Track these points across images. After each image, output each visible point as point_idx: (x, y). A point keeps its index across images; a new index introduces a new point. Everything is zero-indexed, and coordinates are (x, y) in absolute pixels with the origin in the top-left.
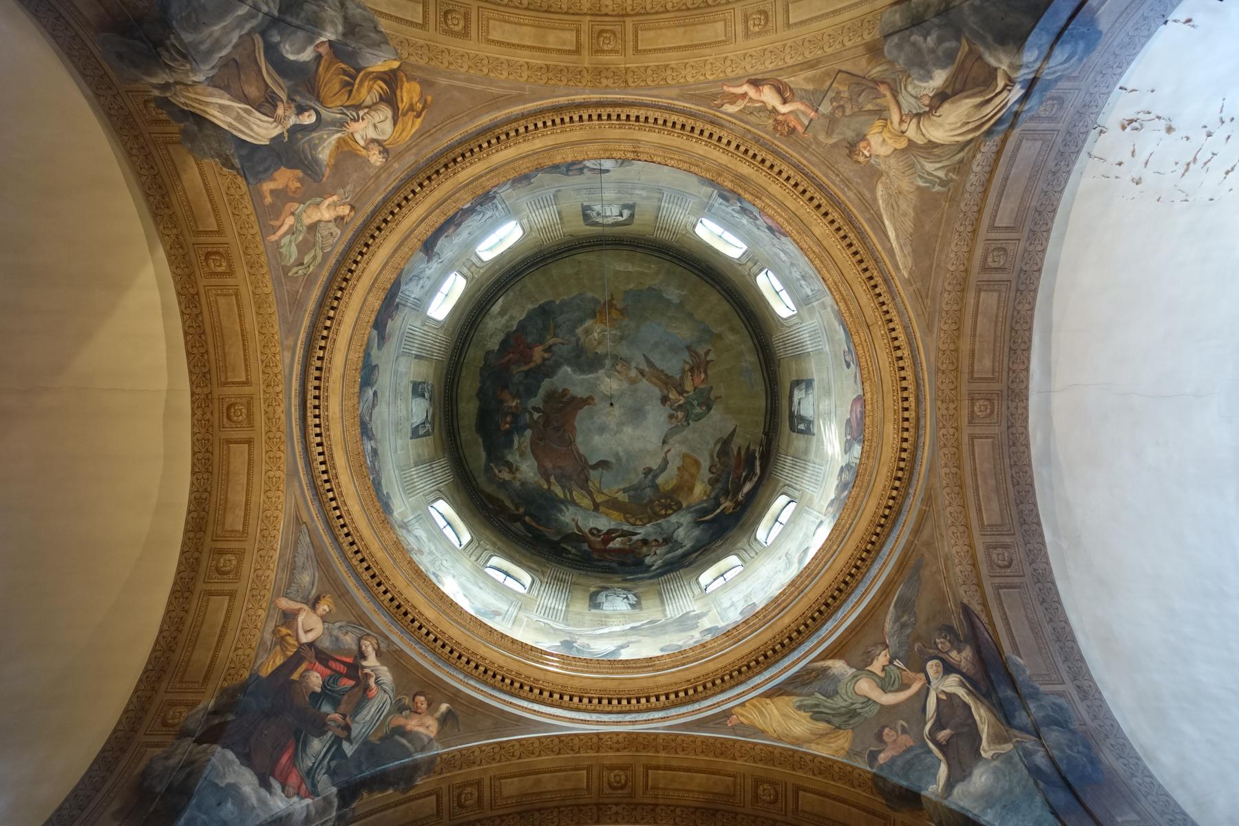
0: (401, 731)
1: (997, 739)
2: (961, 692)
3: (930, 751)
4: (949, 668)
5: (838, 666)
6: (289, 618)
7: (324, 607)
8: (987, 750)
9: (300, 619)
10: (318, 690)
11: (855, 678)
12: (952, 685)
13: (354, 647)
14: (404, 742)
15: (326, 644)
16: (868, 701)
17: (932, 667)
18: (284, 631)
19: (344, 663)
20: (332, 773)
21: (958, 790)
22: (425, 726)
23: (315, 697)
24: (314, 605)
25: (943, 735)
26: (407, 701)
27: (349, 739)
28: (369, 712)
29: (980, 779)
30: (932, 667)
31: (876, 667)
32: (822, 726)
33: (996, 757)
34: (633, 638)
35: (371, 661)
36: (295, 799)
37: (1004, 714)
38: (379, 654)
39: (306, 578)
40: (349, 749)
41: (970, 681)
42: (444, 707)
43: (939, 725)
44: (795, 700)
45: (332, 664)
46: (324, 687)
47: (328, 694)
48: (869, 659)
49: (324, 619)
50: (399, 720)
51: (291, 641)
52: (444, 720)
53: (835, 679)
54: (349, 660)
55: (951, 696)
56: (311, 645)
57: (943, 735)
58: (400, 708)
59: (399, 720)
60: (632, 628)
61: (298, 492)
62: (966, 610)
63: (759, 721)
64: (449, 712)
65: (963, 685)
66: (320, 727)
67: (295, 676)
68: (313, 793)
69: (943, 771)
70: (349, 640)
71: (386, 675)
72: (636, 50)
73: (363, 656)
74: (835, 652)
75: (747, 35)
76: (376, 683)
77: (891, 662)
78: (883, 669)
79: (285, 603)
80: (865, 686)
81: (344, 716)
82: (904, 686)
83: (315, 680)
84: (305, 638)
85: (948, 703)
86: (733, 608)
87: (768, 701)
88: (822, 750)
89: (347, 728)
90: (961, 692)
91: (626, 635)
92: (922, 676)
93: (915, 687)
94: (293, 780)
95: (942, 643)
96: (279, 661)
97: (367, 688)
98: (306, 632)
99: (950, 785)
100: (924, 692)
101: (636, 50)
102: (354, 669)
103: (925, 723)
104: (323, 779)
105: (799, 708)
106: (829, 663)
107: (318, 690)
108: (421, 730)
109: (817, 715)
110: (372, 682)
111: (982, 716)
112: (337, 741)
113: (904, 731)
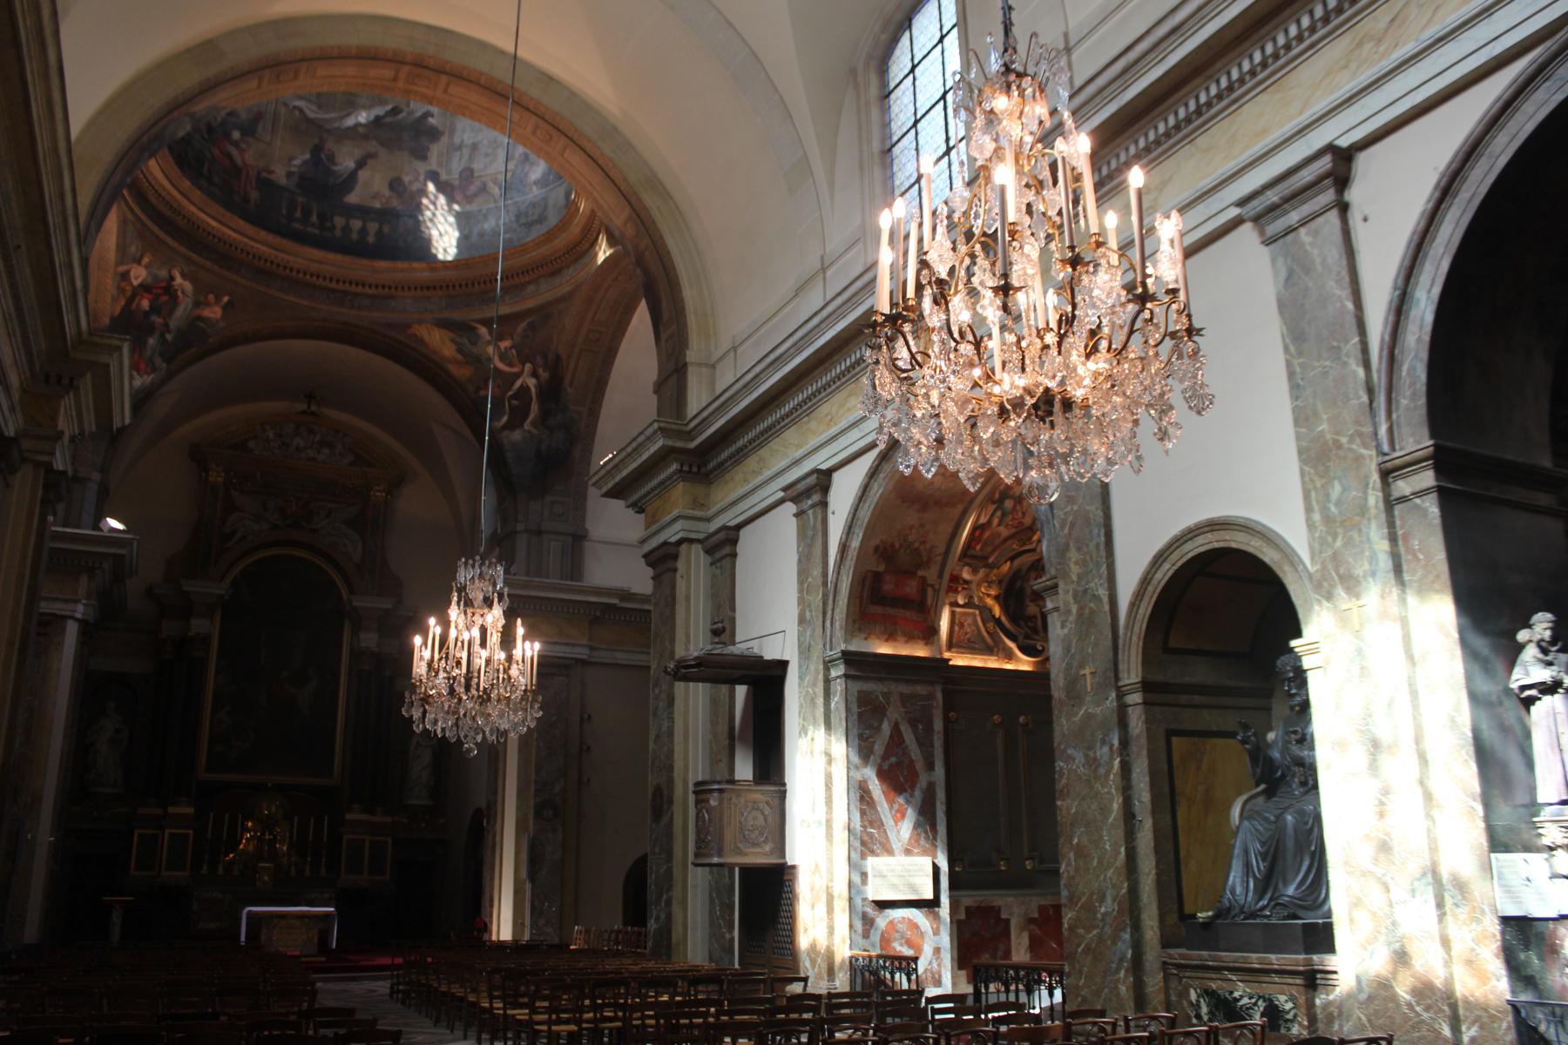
0: (200, 318)
1: (533, 424)
2: (533, 390)
3: (504, 405)
4: (534, 374)
5: (483, 331)
6: (125, 276)
7: (146, 260)
8: (527, 426)
9: (132, 274)
10: (147, 309)
11: (489, 343)
12: (532, 382)
13: (167, 276)
14: (202, 325)
15: (150, 280)
16: (489, 359)
17: (528, 366)
18: (123, 284)
19: (161, 288)
20: (161, 355)
21: (506, 433)
22: (214, 313)
23: (147, 314)
24: (139, 262)
25: (515, 402)
26: (202, 299)
27: (169, 332)
28: (180, 312)
29: (516, 436)
30: (528, 366)
31: (504, 344)
32: (460, 357)
33: (528, 431)
34: (372, 146)
35: (179, 280)
36: (145, 377)
37: (545, 414)
38: (183, 276)
39: (133, 249)
40: (169, 337)
41: (539, 387)
42: (226, 299)
43: (514, 397)
44: (452, 335)
45: (154, 291)
46: (151, 306)
47: (154, 309)
48: (500, 338)
49: (146, 267)
50: (198, 312)
51: (128, 288)
52: (225, 308)
53: (479, 337)
54: (163, 284)
55: (528, 388)
56: (141, 285)
57: (515, 402)
58: (197, 304)
59: (198, 312)
60: (378, 119)
61: (125, 208)
62: (558, 358)
63: (426, 338)
64: (229, 301)
65: (535, 386)
66: (151, 329)
67: (134, 307)
68: (154, 370)
69: (505, 419)
70: (163, 273)
71: (188, 286)
72: (445, 91)
73: (172, 279)
74: (487, 323)
75: (534, 133)
76: (183, 292)
77: (511, 348)
78: (506, 348)
79: (122, 269)
80: (490, 350)
81: (164, 319)
82: (510, 365)
83: (145, 304)
84: (135, 283)
85: (525, 389)
86: (458, 154)
87: (436, 329)
88: (454, 370)
89: (167, 325)
90: (533, 390)
91: (365, 137)
92: (521, 366)
93: (515, 370)
94: (142, 366)
95: (539, 359)
96: (123, 303)
97: (177, 297)
98: (136, 279)
99: (504, 427)
100: (518, 375)
101: (445, 91)
102: (169, 289)
103: (510, 390)
104: (158, 361)
105: (453, 341)
106: (479, 326)
107: (147, 309)
108: (212, 315)
109: (460, 351)
110: (179, 293)
111: (535, 407)
112: (162, 336)
113: (499, 386)
